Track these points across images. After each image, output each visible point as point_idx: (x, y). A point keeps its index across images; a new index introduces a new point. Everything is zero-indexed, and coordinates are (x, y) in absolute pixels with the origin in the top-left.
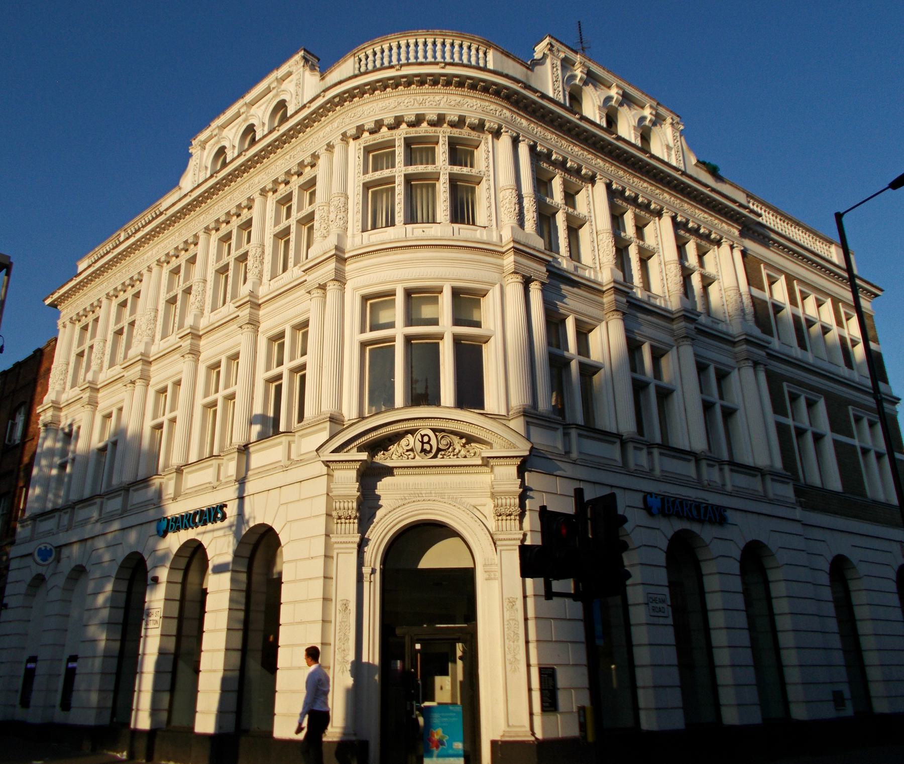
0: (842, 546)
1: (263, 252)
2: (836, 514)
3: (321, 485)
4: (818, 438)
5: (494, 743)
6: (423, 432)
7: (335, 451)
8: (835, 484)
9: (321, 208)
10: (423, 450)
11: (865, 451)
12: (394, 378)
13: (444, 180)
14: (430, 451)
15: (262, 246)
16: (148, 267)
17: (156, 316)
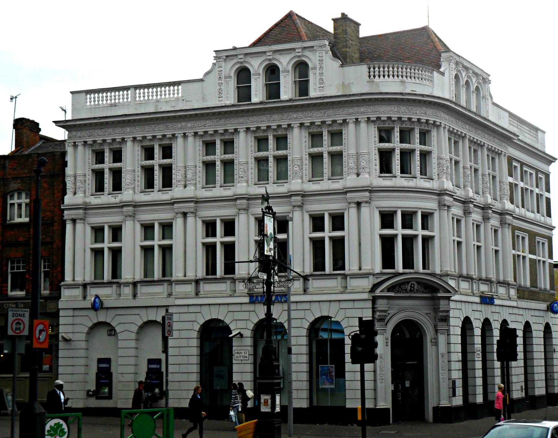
0: (528, 317)
1: (302, 163)
2: (527, 299)
3: (369, 304)
4: (524, 257)
5: (434, 408)
6: (412, 283)
7: (382, 291)
8: (528, 284)
9: (354, 156)
10: (411, 291)
11: (539, 261)
12: (394, 253)
13: (418, 153)
14: (413, 290)
15: (301, 159)
16: (185, 134)
17: (196, 171)
